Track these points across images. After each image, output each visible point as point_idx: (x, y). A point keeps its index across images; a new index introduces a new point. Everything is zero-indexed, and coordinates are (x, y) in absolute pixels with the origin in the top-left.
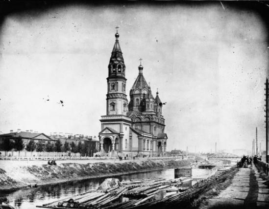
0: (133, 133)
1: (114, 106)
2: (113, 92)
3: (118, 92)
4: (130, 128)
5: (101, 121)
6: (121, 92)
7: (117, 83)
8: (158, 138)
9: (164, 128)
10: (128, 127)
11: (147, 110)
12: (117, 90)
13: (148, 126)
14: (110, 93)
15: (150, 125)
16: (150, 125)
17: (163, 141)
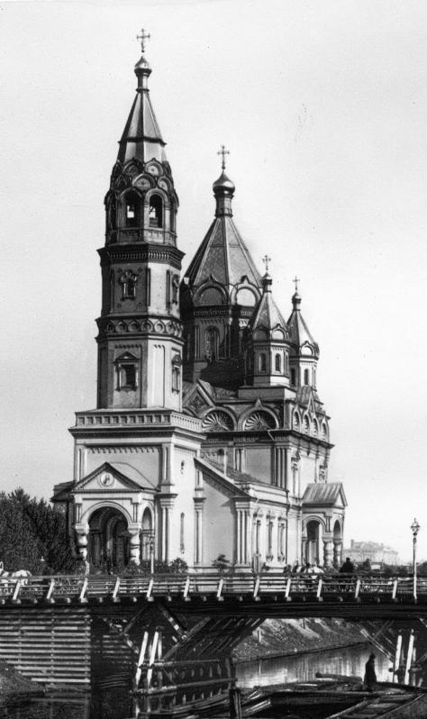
1: (130, 373)
2: (129, 308)
4: (197, 463)
5: (77, 433)
6: (163, 312)
7: (148, 271)
8: (307, 507)
12: (146, 302)
14: (114, 313)
15: (273, 445)
16: (273, 445)
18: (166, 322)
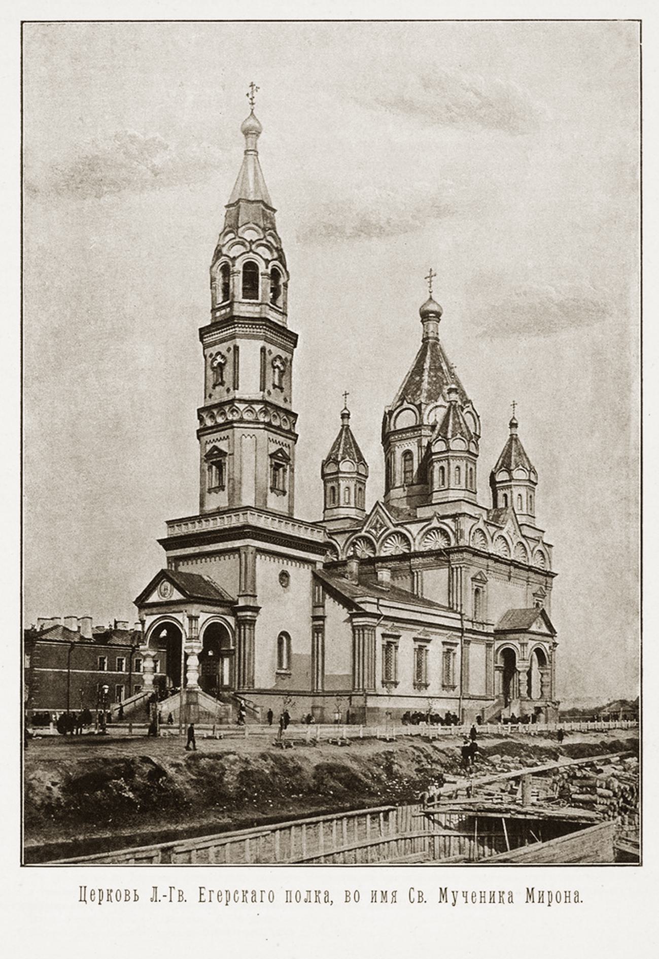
0: (329, 602)
3: (238, 394)
7: (236, 348)
8: (500, 633)
9: (548, 587)
10: (301, 576)
11: (436, 497)
12: (236, 388)
13: (444, 572)
17: (525, 650)
18: (258, 407)
